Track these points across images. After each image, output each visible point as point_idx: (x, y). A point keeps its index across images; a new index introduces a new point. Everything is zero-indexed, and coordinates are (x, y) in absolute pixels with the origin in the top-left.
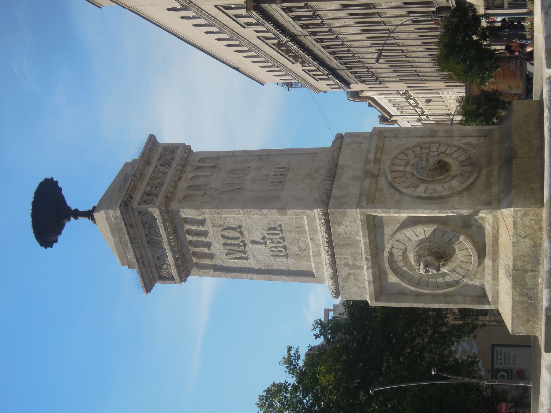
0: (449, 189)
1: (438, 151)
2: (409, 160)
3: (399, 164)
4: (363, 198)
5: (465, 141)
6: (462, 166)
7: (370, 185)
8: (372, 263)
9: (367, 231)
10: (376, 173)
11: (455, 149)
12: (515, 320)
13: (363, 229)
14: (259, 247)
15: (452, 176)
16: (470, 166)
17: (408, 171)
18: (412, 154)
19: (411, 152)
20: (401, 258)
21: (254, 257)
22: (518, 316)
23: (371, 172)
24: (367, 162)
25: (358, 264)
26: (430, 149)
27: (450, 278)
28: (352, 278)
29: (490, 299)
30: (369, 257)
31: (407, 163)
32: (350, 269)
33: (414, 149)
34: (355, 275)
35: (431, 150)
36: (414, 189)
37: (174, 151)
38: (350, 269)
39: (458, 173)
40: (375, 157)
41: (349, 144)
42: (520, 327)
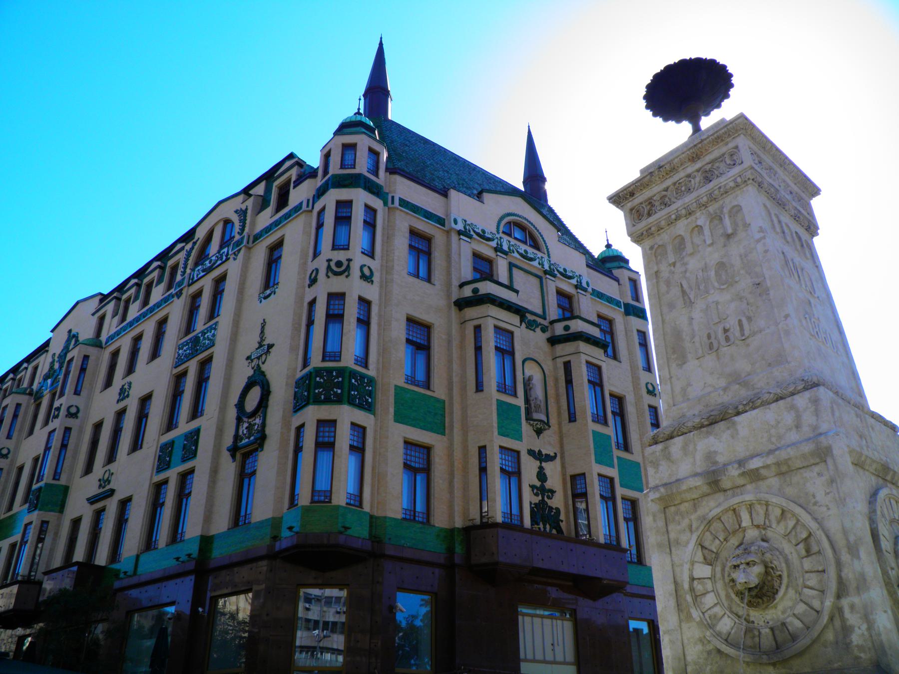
0: (709, 617)
1: (807, 572)
2: (771, 527)
3: (754, 515)
4: (662, 490)
5: (852, 619)
6: (772, 629)
7: (690, 488)
10: (726, 483)
11: (816, 604)
15: (748, 615)
16: (774, 643)
17: (746, 535)
18: (786, 528)
19: (791, 523)
23: (719, 478)
24: (741, 463)
26: (805, 557)
31: (764, 527)
33: (799, 528)
35: (804, 559)
36: (702, 559)
37: (734, 164)
39: (758, 624)
40: (757, 469)
41: (793, 407)
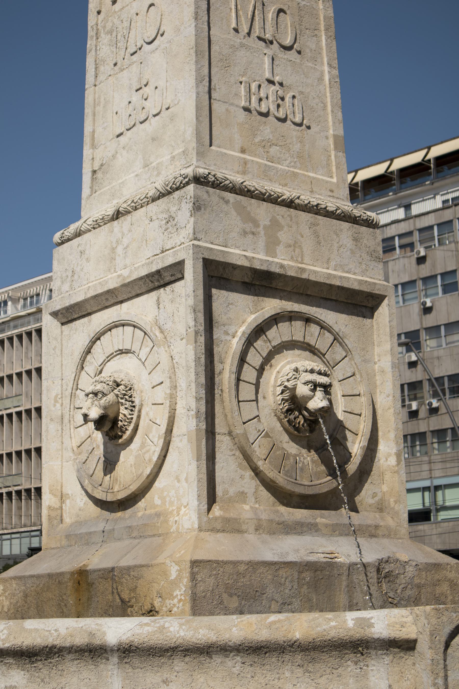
8: (292, 278)
9: (356, 287)
12: (229, 569)
13: (360, 282)
14: (266, 66)
20: (298, 337)
21: (242, 45)
22: (238, 574)
25: (280, 249)
27: (259, 431)
28: (249, 227)
29: (216, 511)
30: (305, 276)
32: (265, 227)
34: (253, 233)
38: (265, 227)
42: (211, 581)
